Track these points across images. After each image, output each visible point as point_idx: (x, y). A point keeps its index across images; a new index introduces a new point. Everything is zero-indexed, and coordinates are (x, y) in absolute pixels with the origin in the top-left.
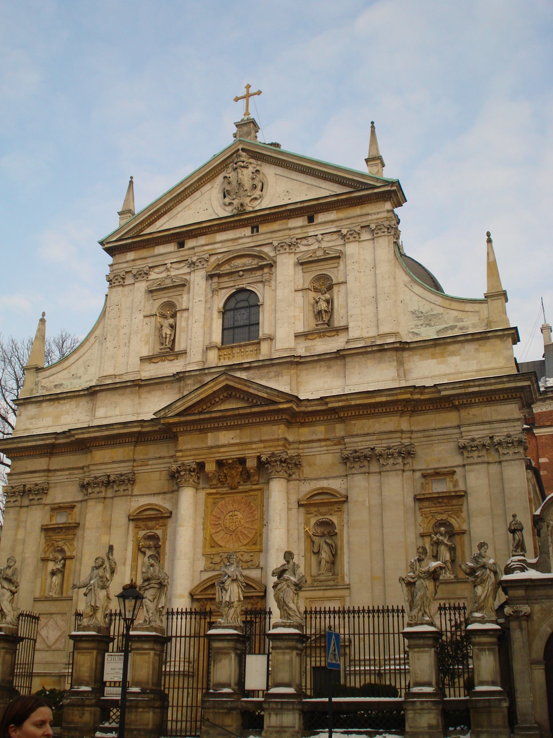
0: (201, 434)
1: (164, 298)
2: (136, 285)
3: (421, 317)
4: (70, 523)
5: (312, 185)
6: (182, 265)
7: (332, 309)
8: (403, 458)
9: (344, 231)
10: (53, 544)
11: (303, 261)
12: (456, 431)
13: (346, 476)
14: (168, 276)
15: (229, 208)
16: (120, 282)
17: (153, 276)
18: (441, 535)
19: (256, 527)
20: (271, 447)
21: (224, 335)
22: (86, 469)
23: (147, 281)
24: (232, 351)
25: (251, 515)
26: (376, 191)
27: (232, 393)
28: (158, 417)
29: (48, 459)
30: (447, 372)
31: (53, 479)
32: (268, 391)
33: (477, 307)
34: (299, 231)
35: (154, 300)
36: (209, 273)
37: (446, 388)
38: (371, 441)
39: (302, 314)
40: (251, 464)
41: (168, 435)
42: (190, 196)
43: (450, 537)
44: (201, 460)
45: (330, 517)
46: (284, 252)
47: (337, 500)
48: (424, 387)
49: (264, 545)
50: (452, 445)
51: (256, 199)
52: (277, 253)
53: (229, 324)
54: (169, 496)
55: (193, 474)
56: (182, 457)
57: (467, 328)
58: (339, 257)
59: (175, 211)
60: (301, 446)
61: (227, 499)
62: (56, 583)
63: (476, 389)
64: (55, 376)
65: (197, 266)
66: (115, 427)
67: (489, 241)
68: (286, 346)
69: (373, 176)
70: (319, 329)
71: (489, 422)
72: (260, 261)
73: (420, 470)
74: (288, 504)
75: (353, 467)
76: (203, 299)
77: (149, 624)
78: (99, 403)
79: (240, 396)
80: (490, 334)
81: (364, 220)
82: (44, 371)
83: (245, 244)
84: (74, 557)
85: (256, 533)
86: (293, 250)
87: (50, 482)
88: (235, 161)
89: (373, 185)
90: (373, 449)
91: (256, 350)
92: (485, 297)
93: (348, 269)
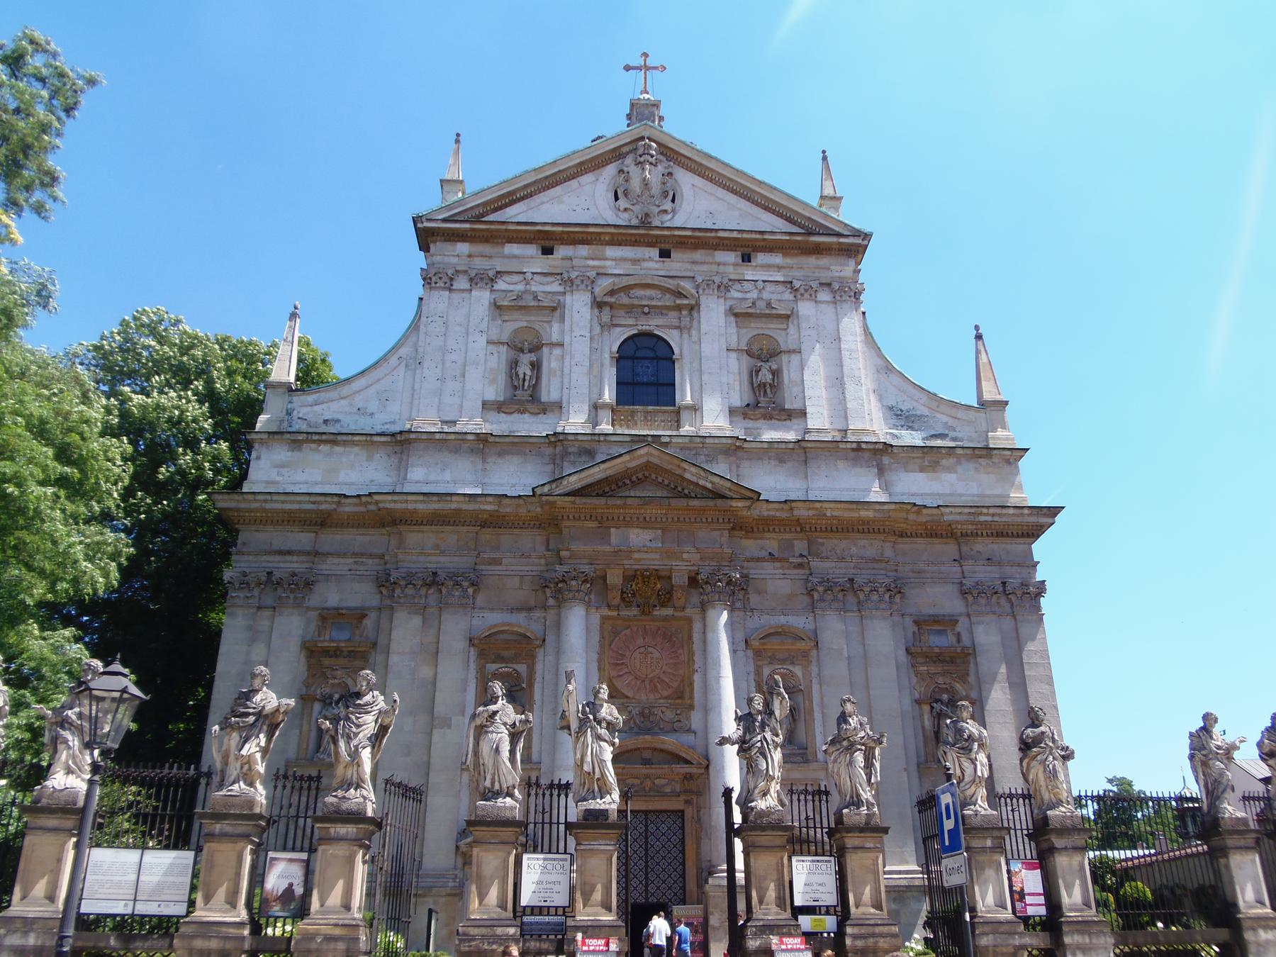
1: (518, 322)
9: (797, 284)
15: (626, 215)
17: (501, 285)
24: (633, 416)
29: (313, 535)
32: (716, 480)
33: (972, 415)
34: (731, 269)
39: (737, 383)
40: (680, 579)
45: (791, 668)
50: (952, 589)
51: (665, 212)
52: (701, 292)
54: (538, 614)
57: (961, 440)
58: (788, 317)
63: (989, 518)
64: (325, 406)
66: (454, 498)
67: (979, 337)
78: (413, 460)
80: (995, 452)
83: (650, 269)
85: (683, 681)
90: (851, 580)
93: (802, 334)
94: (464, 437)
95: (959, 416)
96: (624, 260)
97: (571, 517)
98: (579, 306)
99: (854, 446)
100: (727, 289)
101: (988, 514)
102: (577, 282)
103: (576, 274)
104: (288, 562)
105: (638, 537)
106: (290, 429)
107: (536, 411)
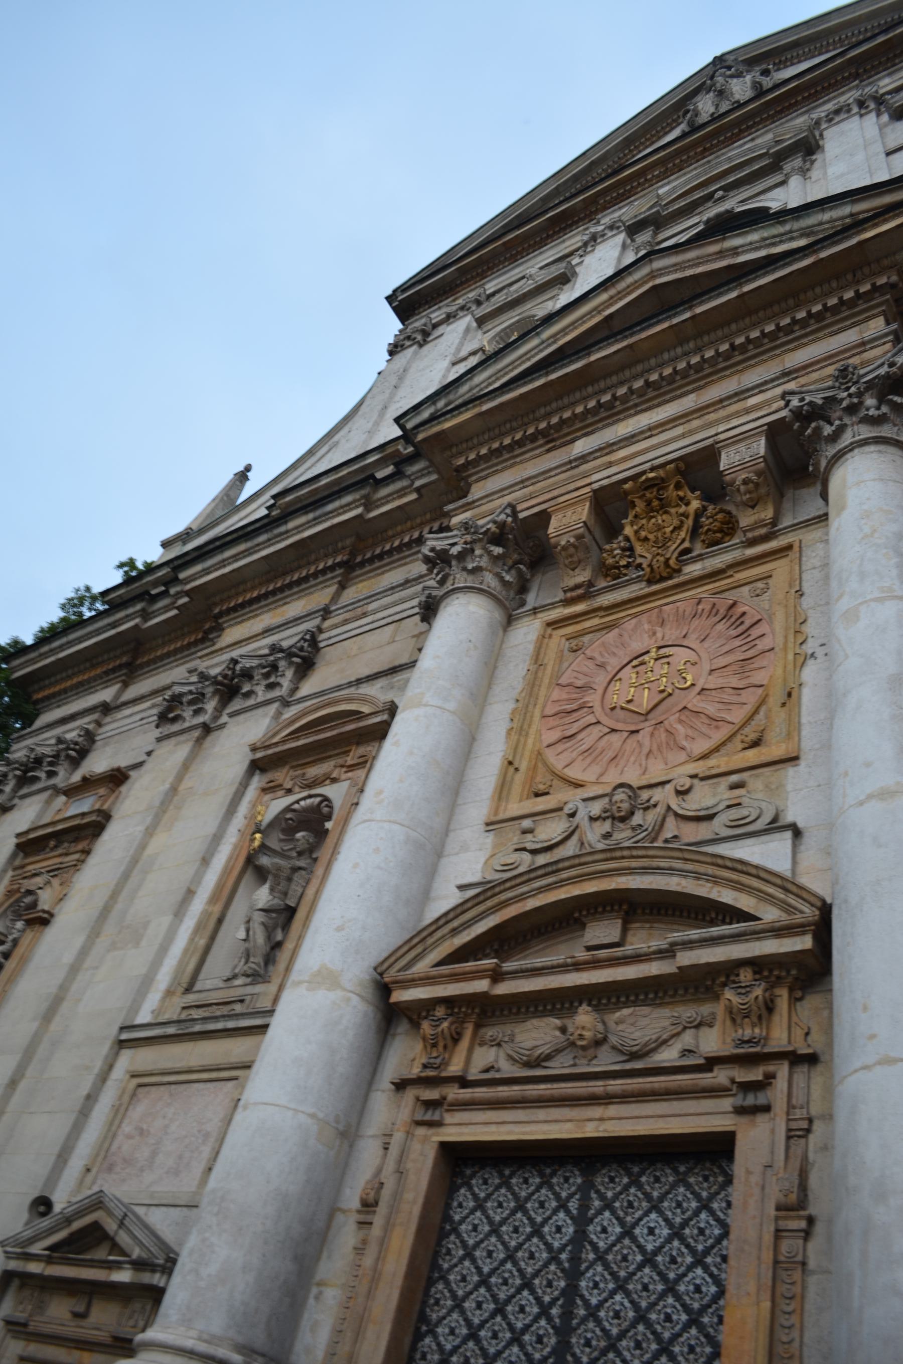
0: (548, 451)
19: (759, 677)
25: (737, 642)
28: (409, 426)
36: (627, 224)
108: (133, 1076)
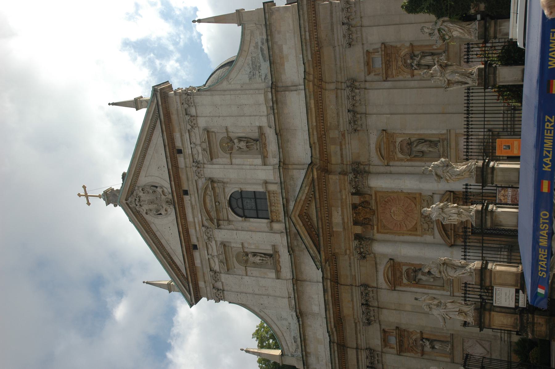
0: (333, 236)
2: (223, 281)
3: (253, 73)
4: (396, 334)
5: (154, 150)
6: (209, 246)
7: (246, 138)
8: (356, 88)
9: (189, 127)
10: (411, 347)
11: (210, 158)
12: (337, 48)
13: (367, 130)
14: (217, 256)
15: (169, 210)
16: (220, 293)
17: (217, 268)
18: (413, 62)
20: (345, 185)
21: (262, 217)
22: (356, 321)
23: (220, 273)
26: (160, 103)
27: (304, 212)
28: (320, 267)
29: (348, 349)
30: (294, 55)
31: (363, 346)
32: (304, 185)
33: (247, 32)
34: (187, 160)
35: (234, 268)
36: (217, 227)
37: (306, 56)
38: (342, 112)
39: (249, 160)
40: (357, 200)
41: (334, 260)
42: (159, 240)
43: (415, 56)
44: (353, 236)
46: (202, 172)
47: (385, 138)
48: (305, 72)
49: (416, 192)
51: (163, 191)
52: (203, 177)
53: (254, 213)
54: (378, 260)
55: (363, 242)
56: (350, 250)
57: (263, 39)
58: (208, 132)
59: (170, 251)
60: (345, 163)
61: (382, 218)
62: (440, 345)
63: (307, 34)
64: (288, 342)
65: (211, 235)
66: (326, 299)
68: (271, 172)
69: (149, 105)
70: (260, 148)
71: (332, 25)
72: (208, 190)
73: (365, 76)
74: (386, 173)
75: (361, 125)
76: (235, 232)
77: (472, 272)
79: (307, 207)
80: (268, 23)
81: (181, 113)
82: (284, 350)
83: (195, 201)
84: (421, 332)
85: (407, 197)
86: (202, 165)
87: (365, 348)
88: (135, 205)
89: (156, 105)
90: (349, 111)
91: (274, 194)
92: (240, 25)
94: (296, 290)
95: (249, 40)
96: (193, 213)
97: (330, 250)
98: (221, 235)
99: (275, 105)
100: (198, 162)
101: (305, 35)
102: (209, 235)
103: (205, 236)
104: (362, 359)
105: (337, 218)
106: (301, 356)
107: (278, 255)
108: (459, 291)
